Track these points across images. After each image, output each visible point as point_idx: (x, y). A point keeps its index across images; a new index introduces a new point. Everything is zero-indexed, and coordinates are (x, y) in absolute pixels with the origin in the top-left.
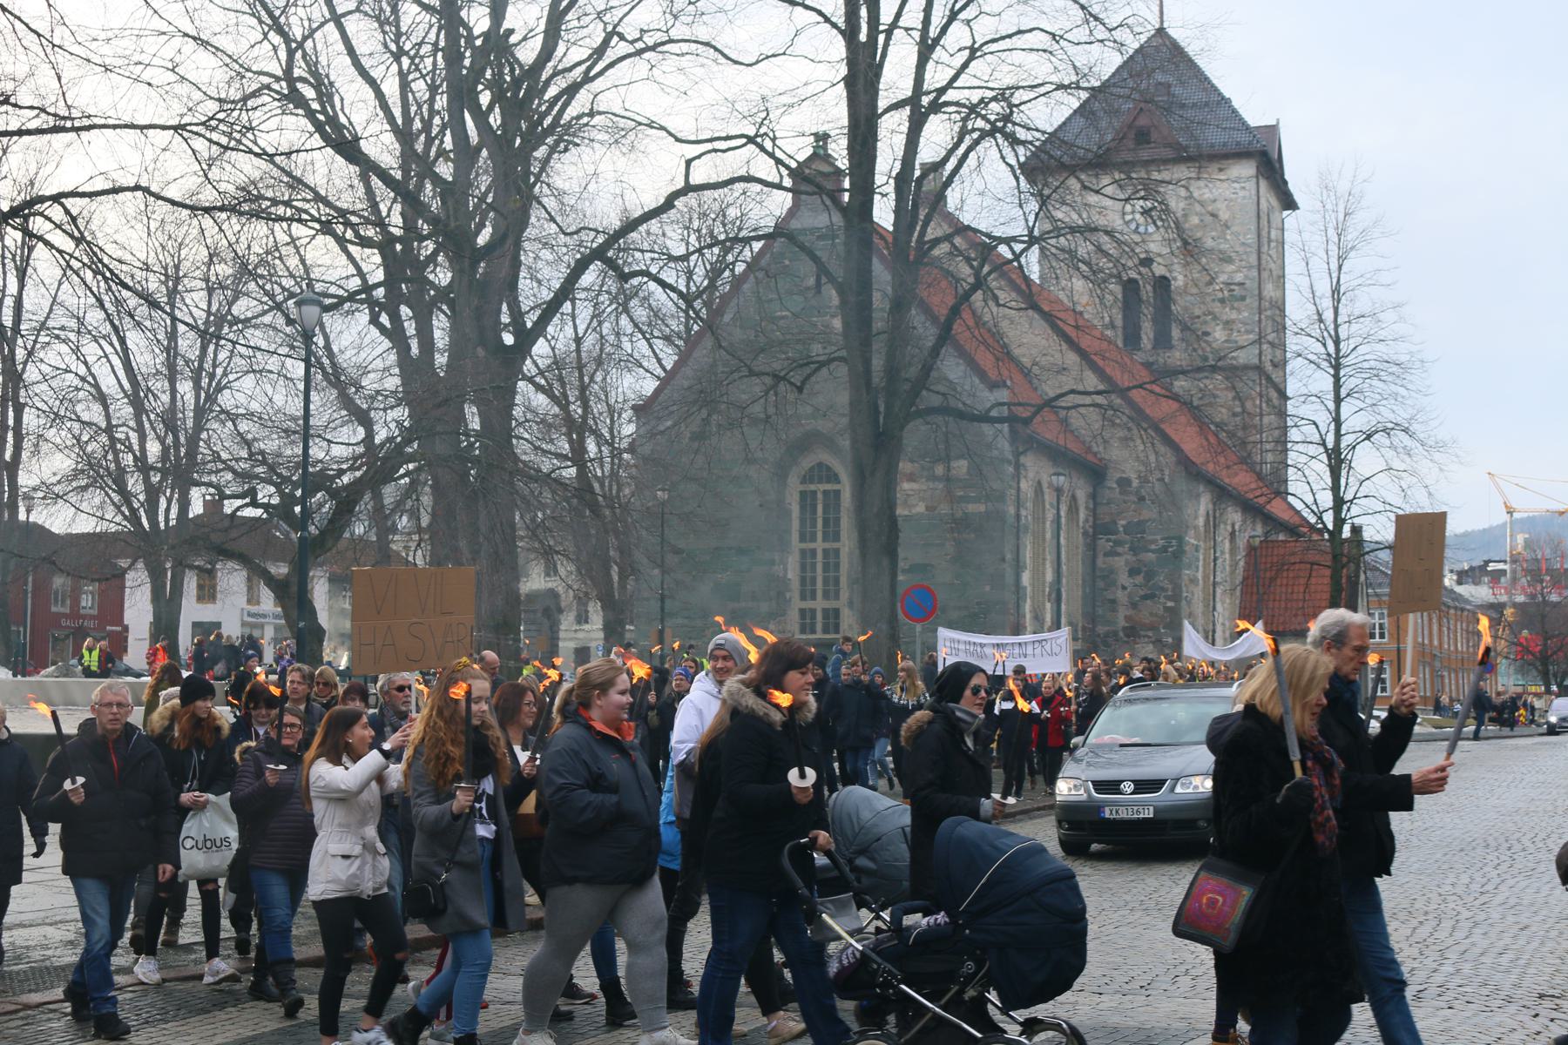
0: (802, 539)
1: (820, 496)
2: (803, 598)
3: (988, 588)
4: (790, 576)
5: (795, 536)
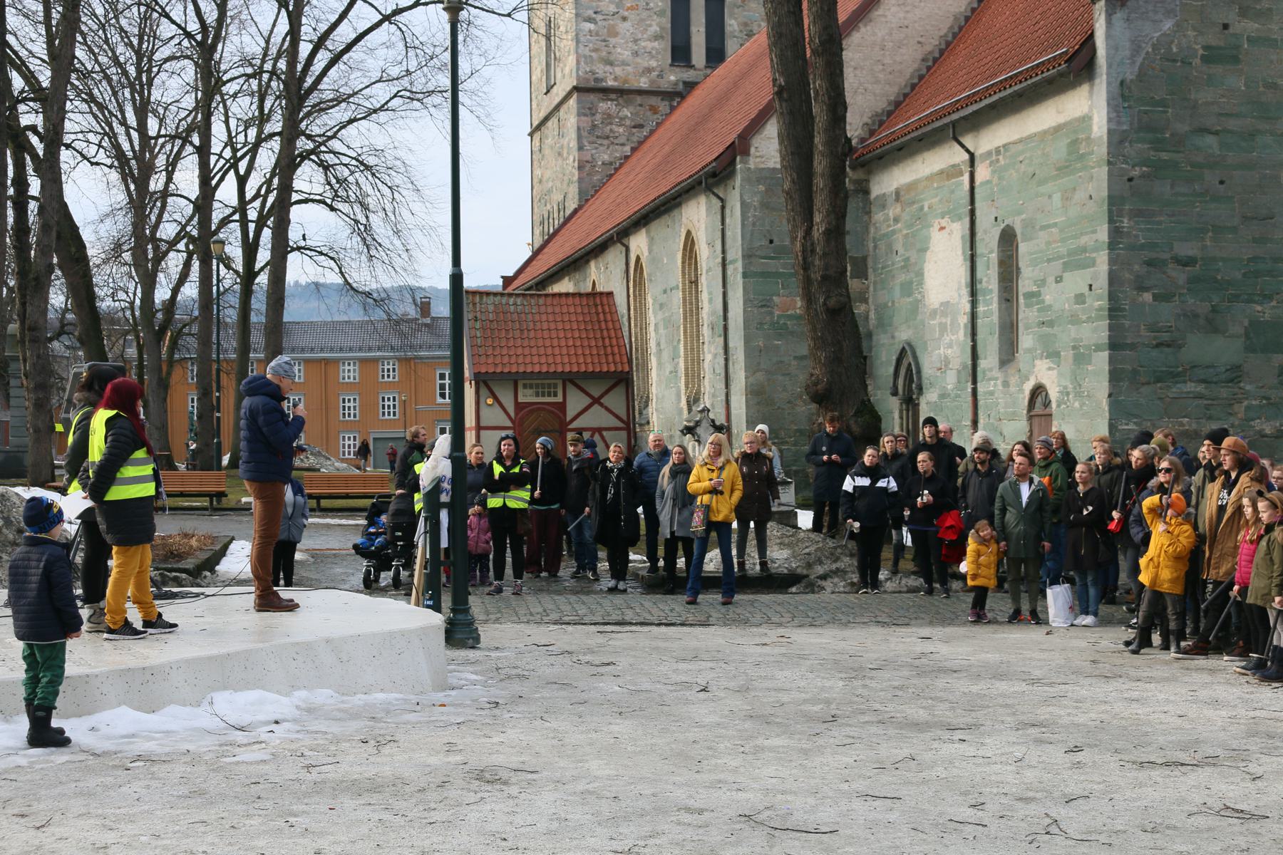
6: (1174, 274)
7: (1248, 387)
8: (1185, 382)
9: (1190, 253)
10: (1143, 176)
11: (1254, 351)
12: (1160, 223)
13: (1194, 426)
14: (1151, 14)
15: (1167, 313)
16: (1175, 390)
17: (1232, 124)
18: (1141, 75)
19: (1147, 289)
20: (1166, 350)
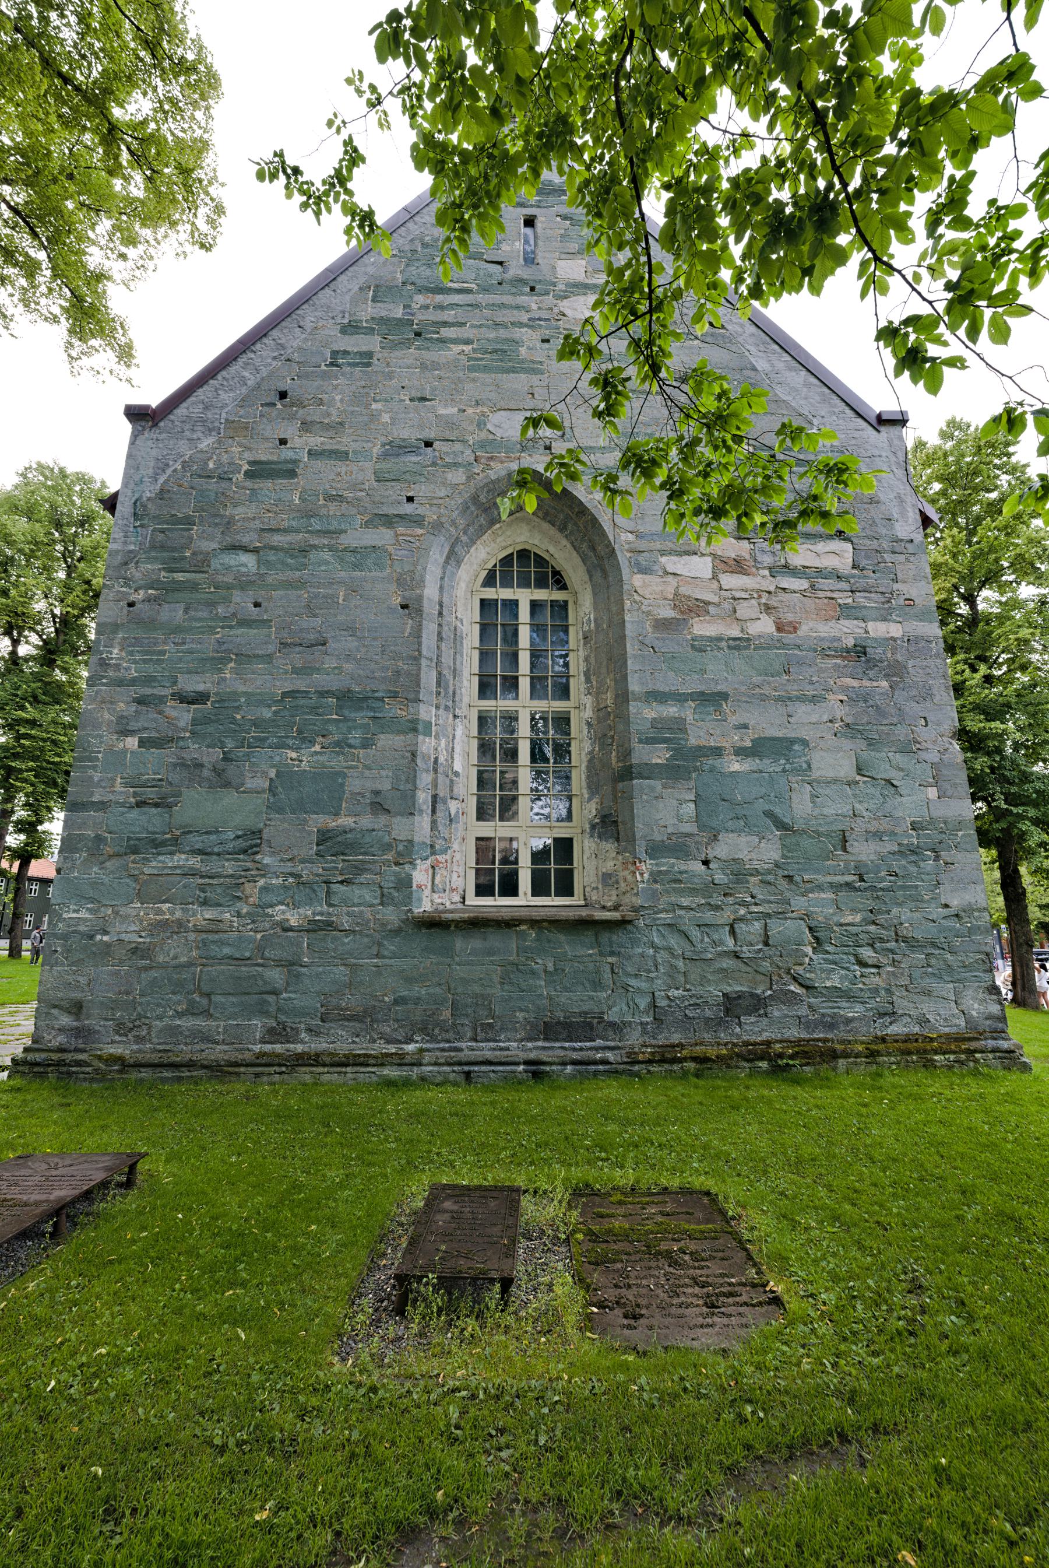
0: (485, 688)
1: (524, 613)
2: (482, 814)
3: (932, 793)
4: (458, 766)
5: (469, 686)
6: (174, 714)
7: (267, 860)
8: (172, 853)
9: (201, 687)
10: (148, 600)
11: (280, 811)
13: (178, 914)
14: (187, 433)
15: (155, 764)
16: (153, 866)
17: (277, 539)
18: (162, 494)
19: (132, 733)
20: (154, 811)
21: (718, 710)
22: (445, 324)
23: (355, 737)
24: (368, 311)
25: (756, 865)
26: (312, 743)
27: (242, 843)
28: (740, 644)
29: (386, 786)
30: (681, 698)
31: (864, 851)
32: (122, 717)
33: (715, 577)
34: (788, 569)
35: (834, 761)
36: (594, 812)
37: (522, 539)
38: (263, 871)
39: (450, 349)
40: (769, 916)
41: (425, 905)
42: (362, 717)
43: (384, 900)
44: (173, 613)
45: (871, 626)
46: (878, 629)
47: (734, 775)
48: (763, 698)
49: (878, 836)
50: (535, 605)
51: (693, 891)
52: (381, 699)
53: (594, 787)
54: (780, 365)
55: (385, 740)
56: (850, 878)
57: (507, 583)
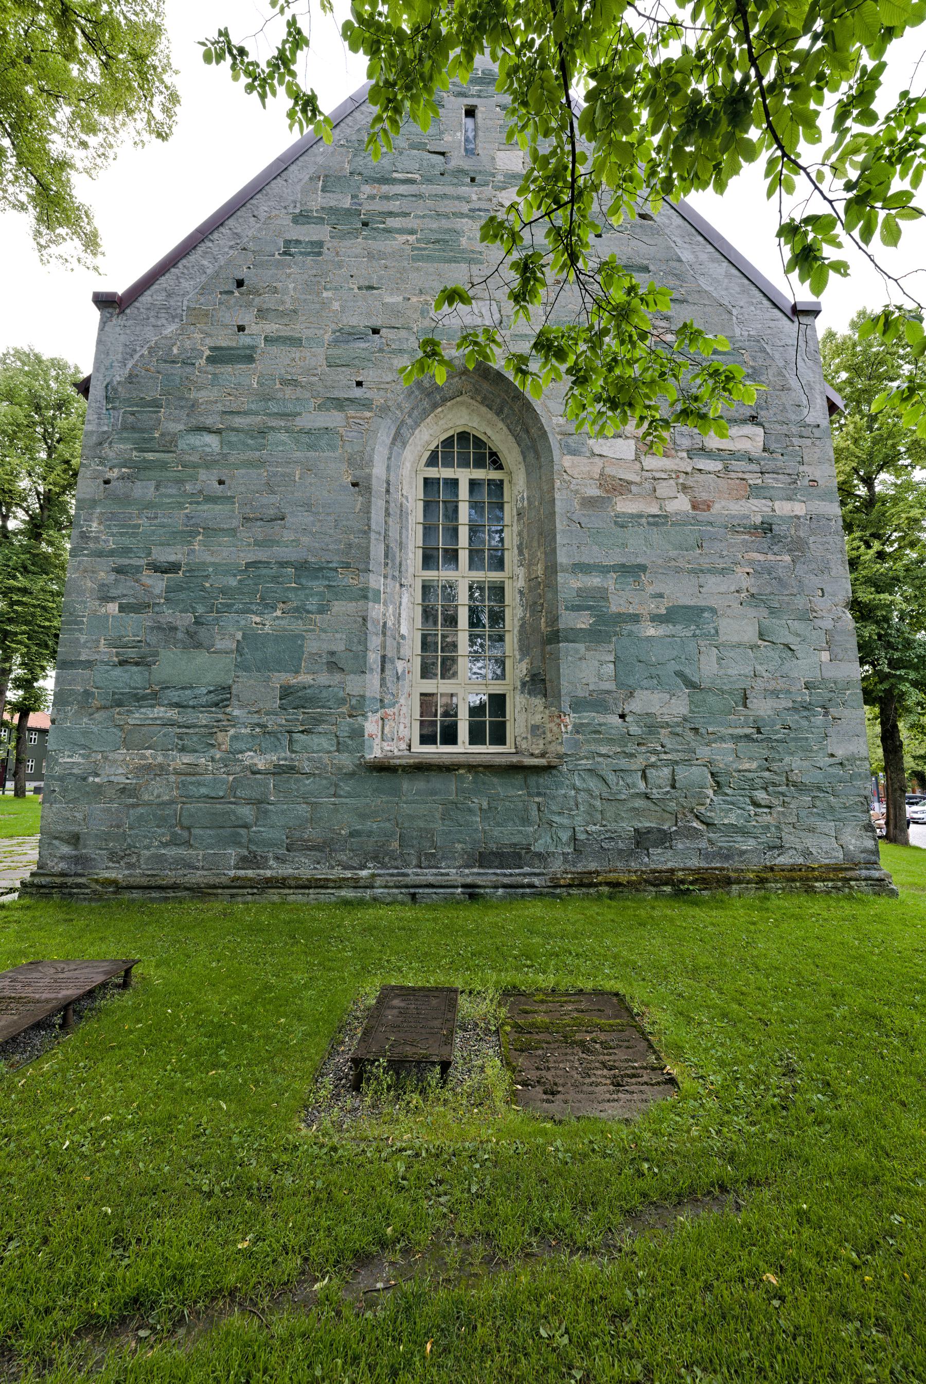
0: (429, 560)
1: (464, 491)
2: (426, 672)
3: (825, 656)
4: (404, 630)
5: (413, 558)
6: (149, 582)
7: (236, 712)
8: (153, 706)
9: (172, 558)
10: (122, 478)
11: (247, 669)
12: (137, 526)
13: (160, 759)
14: (152, 320)
15: (134, 627)
16: (136, 717)
17: (238, 421)
18: (131, 378)
19: (113, 599)
20: (135, 669)
21: (637, 581)
22: (390, 214)
23: (312, 603)
24: (318, 201)
25: (666, 718)
26: (274, 608)
27: (214, 698)
28: (658, 521)
29: (340, 647)
30: (604, 570)
31: (762, 707)
32: (103, 585)
33: (637, 459)
34: (704, 451)
35: (739, 627)
36: (525, 672)
37: (463, 422)
38: (233, 722)
39: (395, 239)
40: (676, 763)
41: (376, 751)
42: (318, 585)
43: (340, 747)
44: (144, 490)
45: (777, 504)
46: (784, 508)
47: (649, 639)
48: (678, 570)
49: (775, 694)
50: (473, 484)
51: (610, 741)
52: (335, 570)
53: (524, 649)
54: (703, 257)
55: (339, 607)
56: (748, 731)
57: (448, 463)
